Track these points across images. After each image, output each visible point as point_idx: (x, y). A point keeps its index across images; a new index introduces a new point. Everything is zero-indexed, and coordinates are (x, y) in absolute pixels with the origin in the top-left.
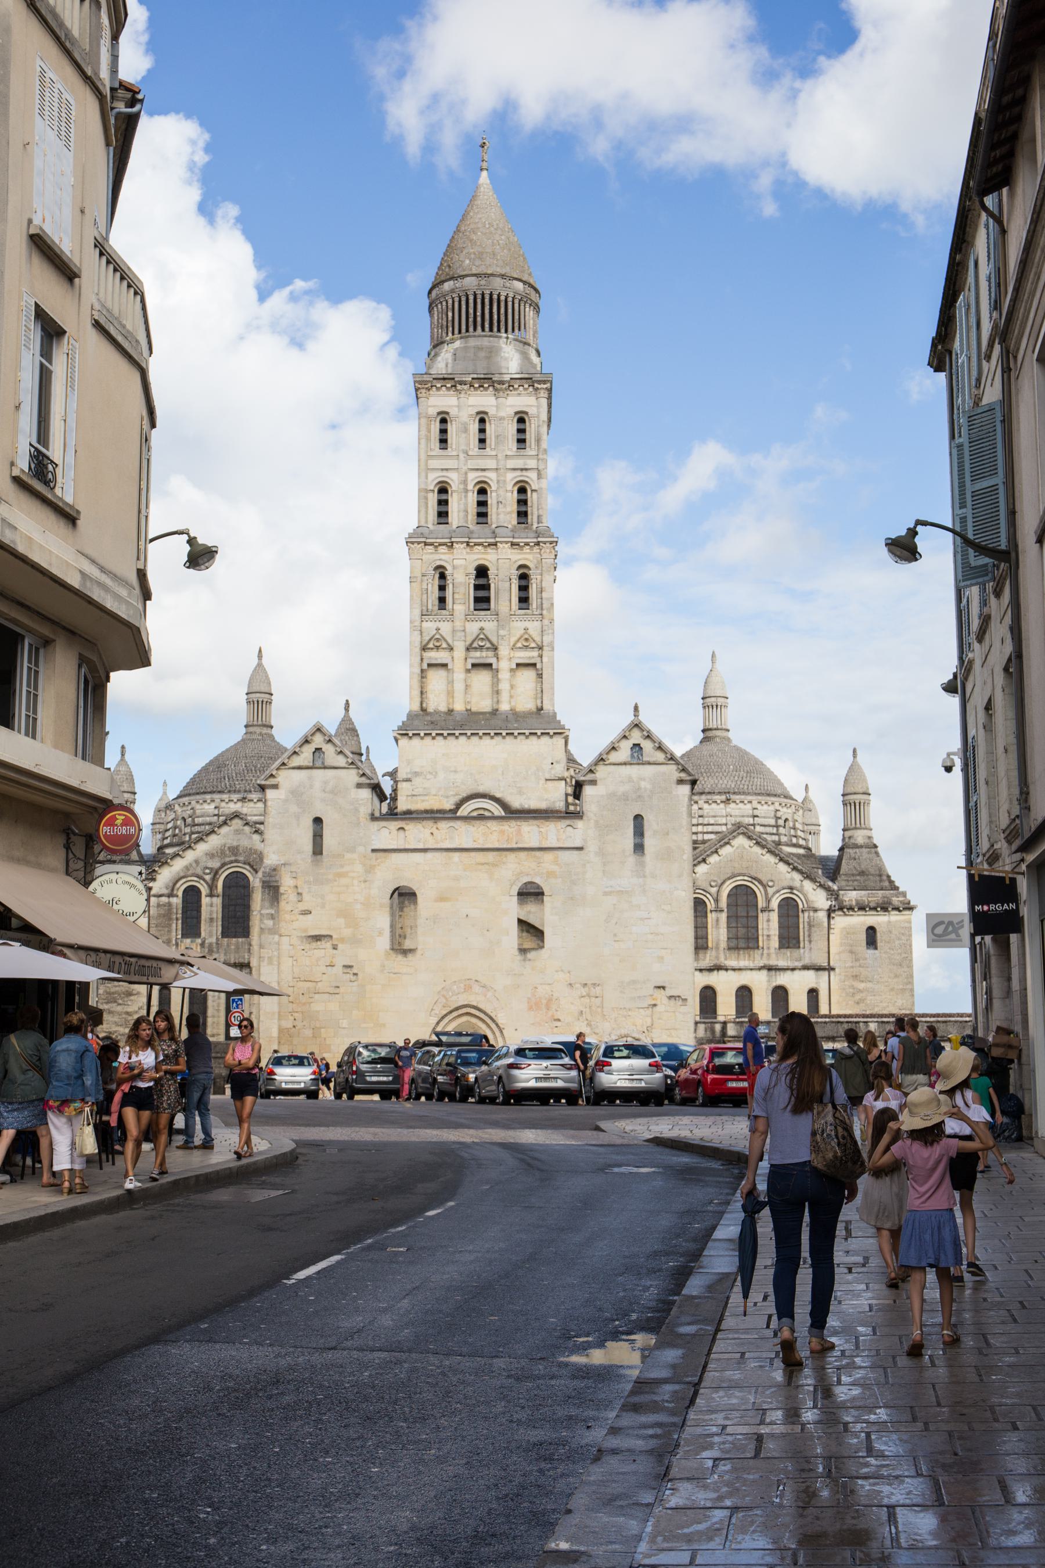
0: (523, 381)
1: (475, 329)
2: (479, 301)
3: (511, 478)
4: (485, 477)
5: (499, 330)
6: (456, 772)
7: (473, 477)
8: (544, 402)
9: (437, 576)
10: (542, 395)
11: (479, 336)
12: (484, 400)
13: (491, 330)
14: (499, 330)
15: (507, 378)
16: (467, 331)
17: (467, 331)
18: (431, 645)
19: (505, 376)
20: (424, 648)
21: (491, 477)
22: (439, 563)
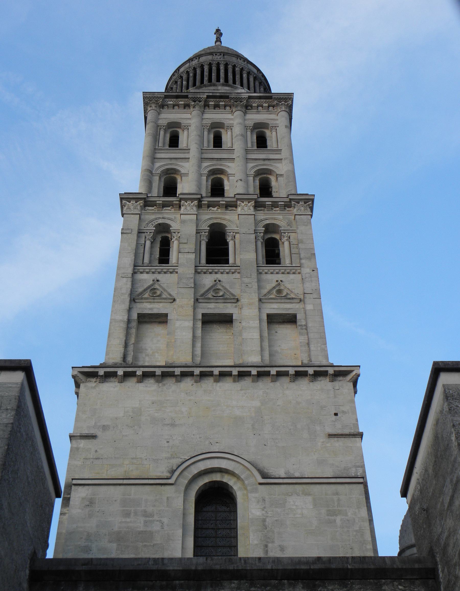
0: (262, 100)
4: (221, 165)
5: (234, 82)
6: (173, 425)
9: (159, 239)
11: (214, 85)
14: (234, 82)
18: (146, 296)
19: (242, 94)
20: (133, 300)
22: (160, 221)
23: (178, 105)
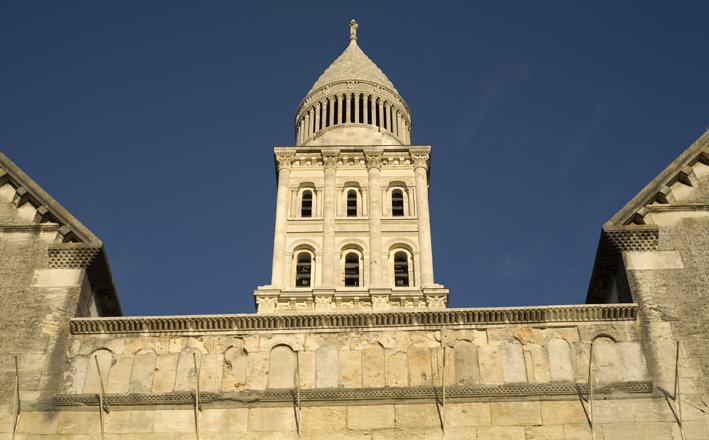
1: (344, 121)
2: (349, 102)
3: (387, 241)
5: (370, 122)
7: (341, 240)
8: (423, 172)
10: (420, 164)
12: (358, 172)
13: (361, 121)
15: (381, 149)
16: (336, 122)
17: (336, 122)
21: (363, 240)
23: (310, 160)
